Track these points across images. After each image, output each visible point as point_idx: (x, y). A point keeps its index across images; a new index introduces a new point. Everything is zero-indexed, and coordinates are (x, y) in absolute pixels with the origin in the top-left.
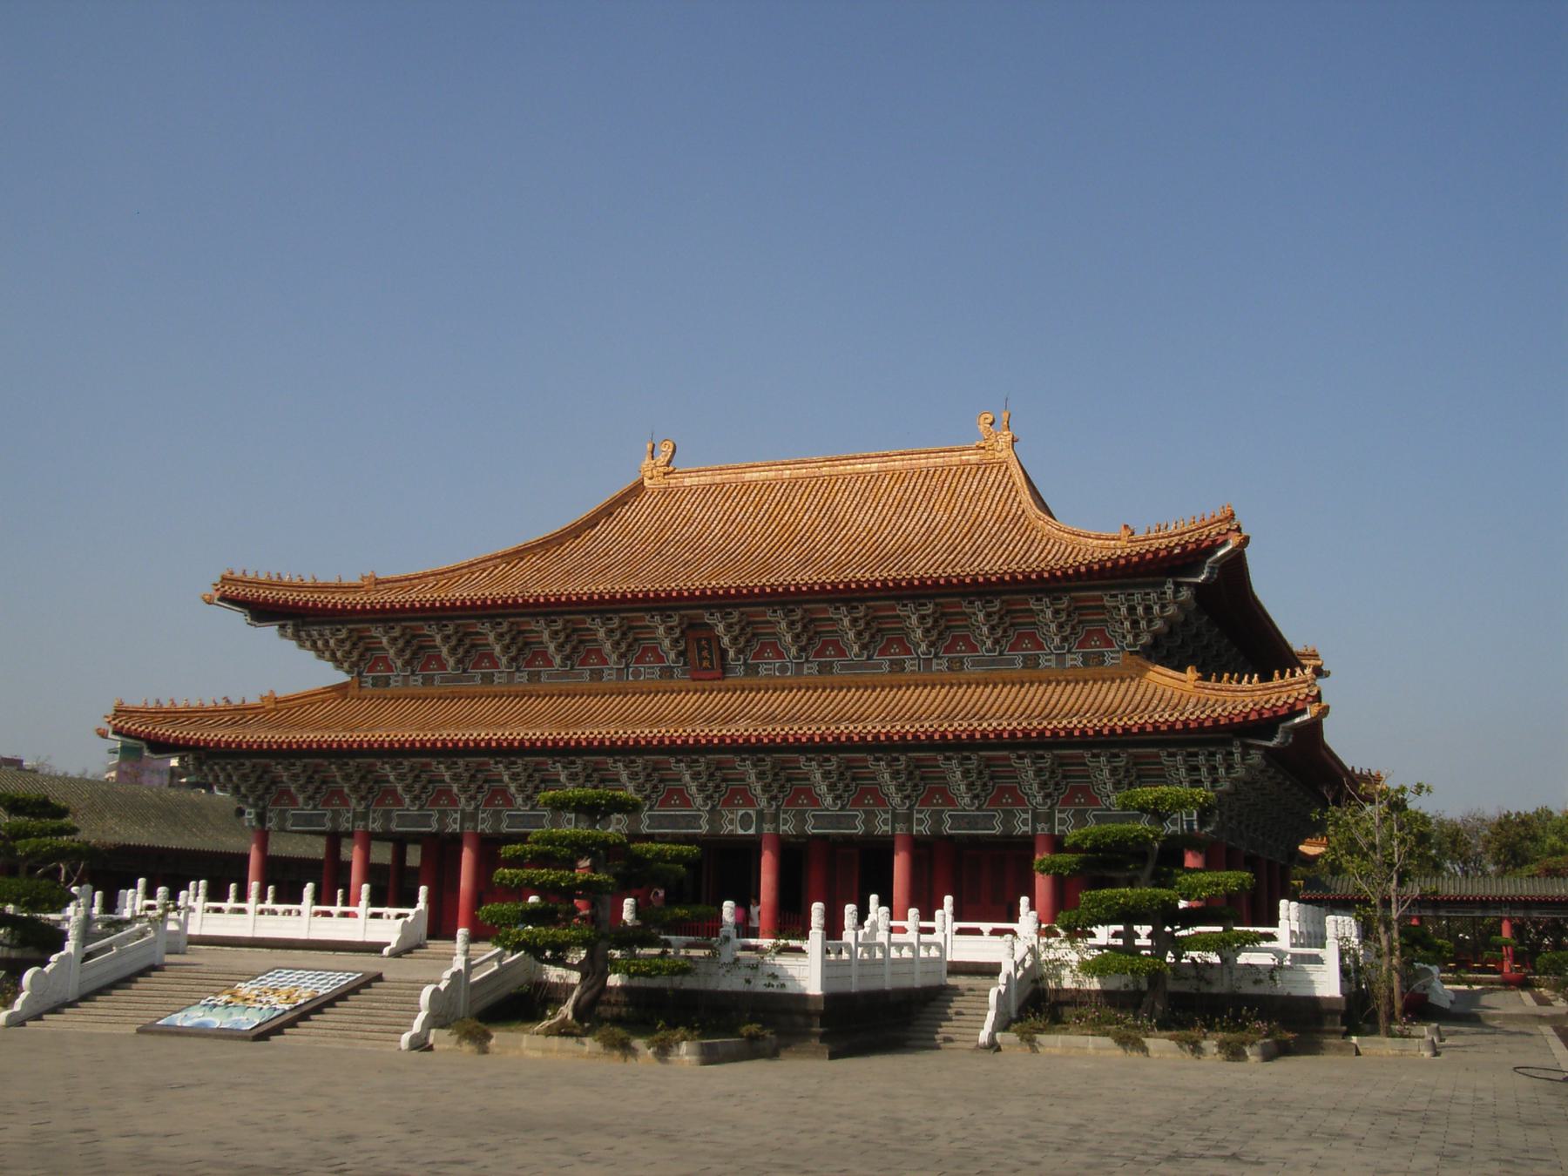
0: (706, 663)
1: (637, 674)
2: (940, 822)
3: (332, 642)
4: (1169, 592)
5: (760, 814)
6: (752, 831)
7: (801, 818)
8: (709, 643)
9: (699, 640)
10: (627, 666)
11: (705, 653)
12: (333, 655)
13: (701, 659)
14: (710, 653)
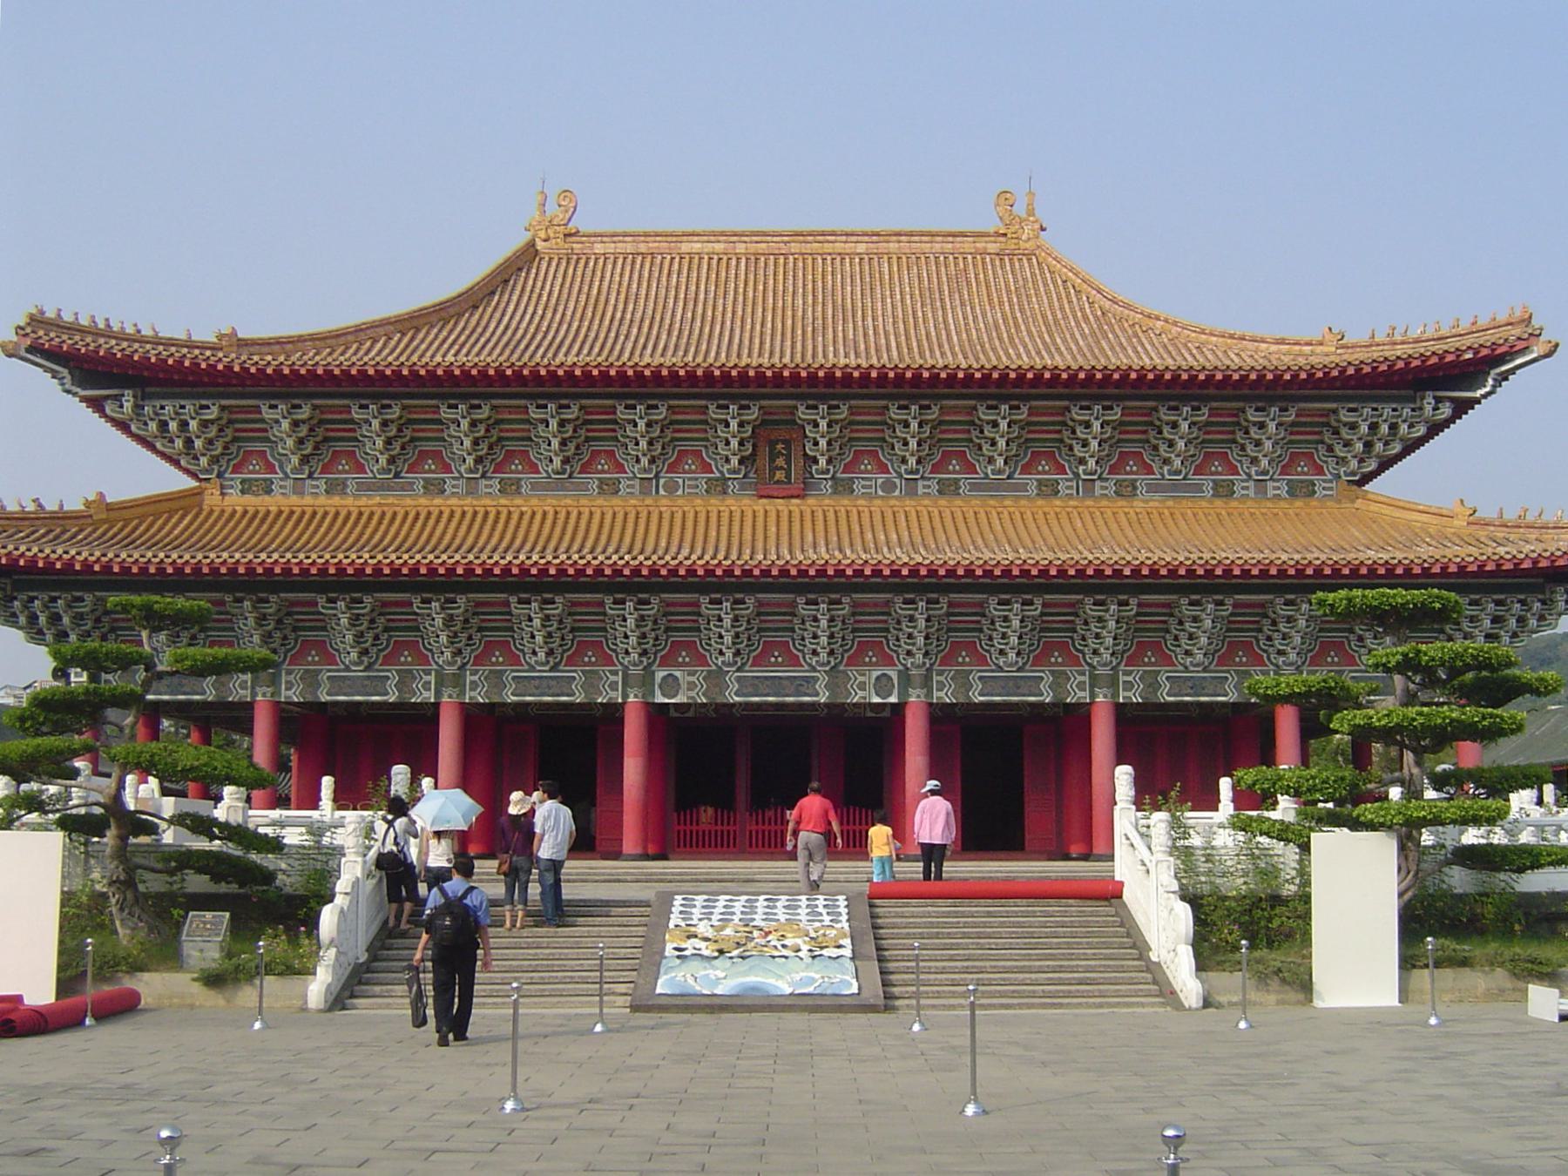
0: (779, 475)
1: (671, 488)
2: (1154, 686)
3: (193, 425)
4: (1428, 409)
5: (905, 677)
6: (893, 699)
7: (963, 681)
8: (787, 443)
9: (772, 444)
10: (657, 476)
11: (780, 462)
12: (189, 443)
13: (773, 470)
14: (788, 462)
